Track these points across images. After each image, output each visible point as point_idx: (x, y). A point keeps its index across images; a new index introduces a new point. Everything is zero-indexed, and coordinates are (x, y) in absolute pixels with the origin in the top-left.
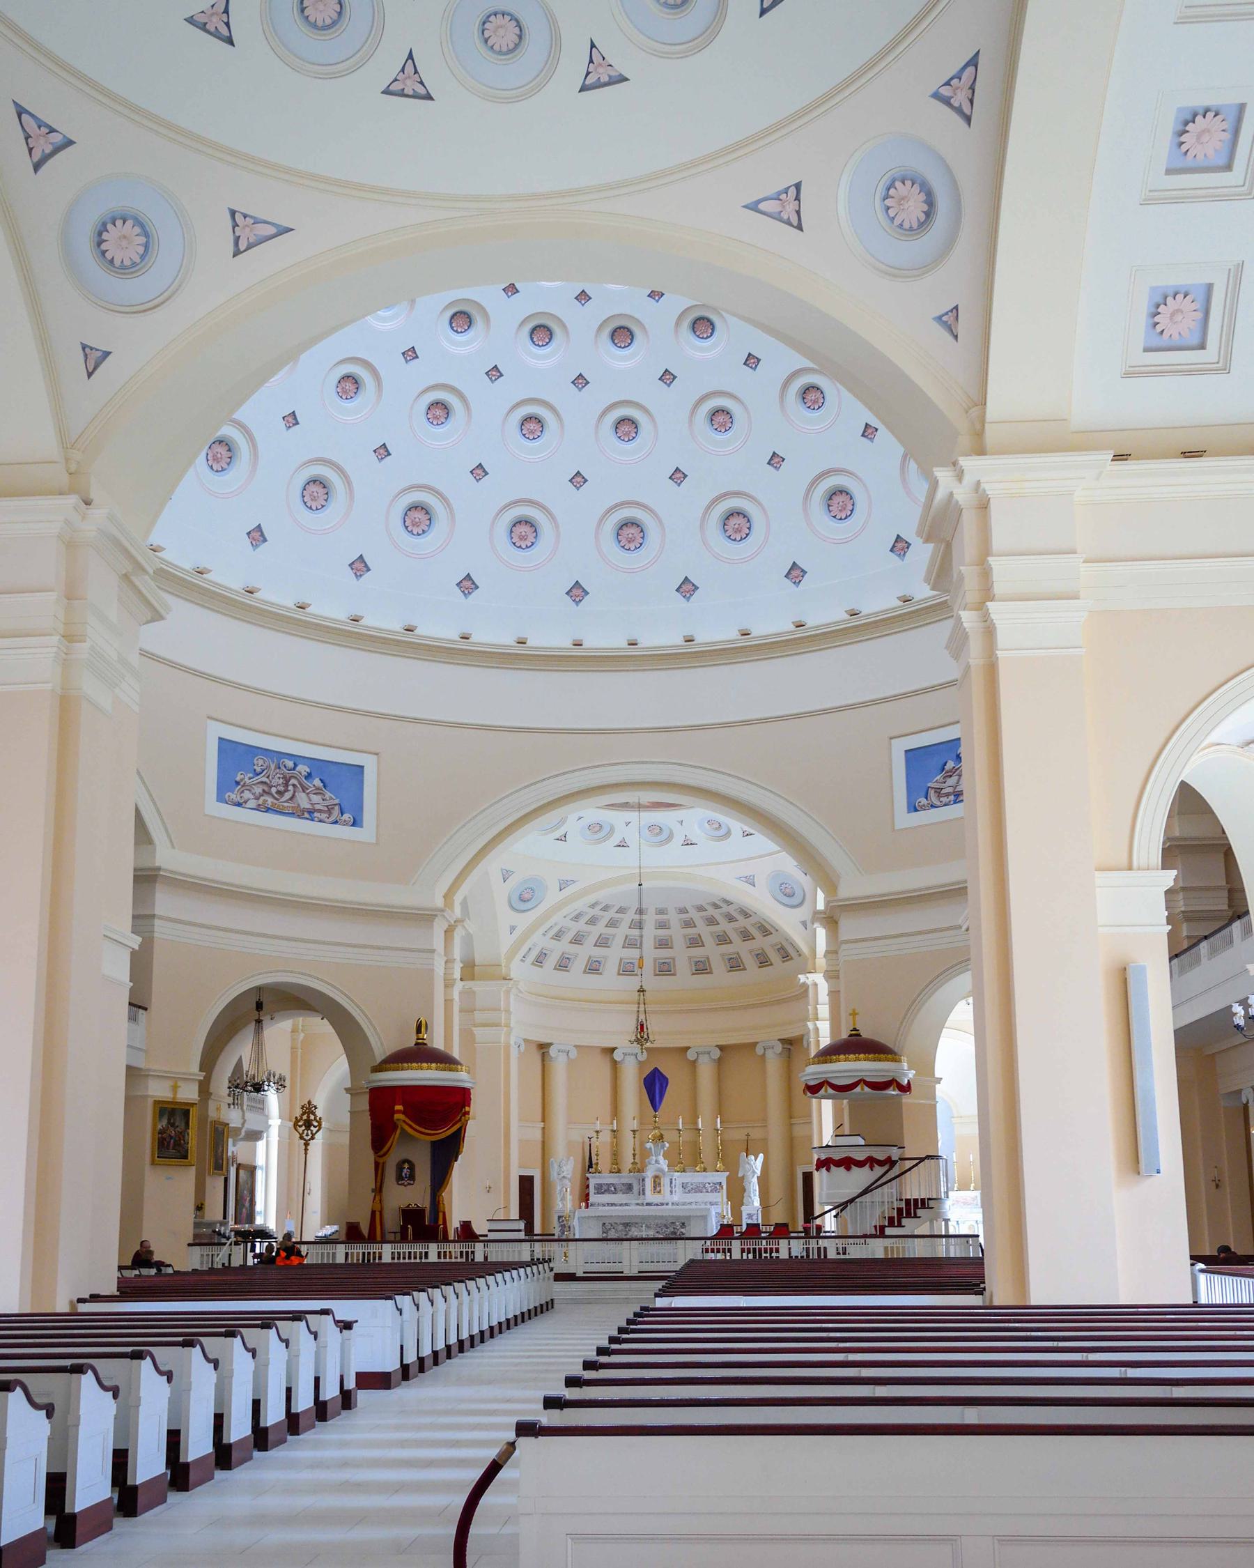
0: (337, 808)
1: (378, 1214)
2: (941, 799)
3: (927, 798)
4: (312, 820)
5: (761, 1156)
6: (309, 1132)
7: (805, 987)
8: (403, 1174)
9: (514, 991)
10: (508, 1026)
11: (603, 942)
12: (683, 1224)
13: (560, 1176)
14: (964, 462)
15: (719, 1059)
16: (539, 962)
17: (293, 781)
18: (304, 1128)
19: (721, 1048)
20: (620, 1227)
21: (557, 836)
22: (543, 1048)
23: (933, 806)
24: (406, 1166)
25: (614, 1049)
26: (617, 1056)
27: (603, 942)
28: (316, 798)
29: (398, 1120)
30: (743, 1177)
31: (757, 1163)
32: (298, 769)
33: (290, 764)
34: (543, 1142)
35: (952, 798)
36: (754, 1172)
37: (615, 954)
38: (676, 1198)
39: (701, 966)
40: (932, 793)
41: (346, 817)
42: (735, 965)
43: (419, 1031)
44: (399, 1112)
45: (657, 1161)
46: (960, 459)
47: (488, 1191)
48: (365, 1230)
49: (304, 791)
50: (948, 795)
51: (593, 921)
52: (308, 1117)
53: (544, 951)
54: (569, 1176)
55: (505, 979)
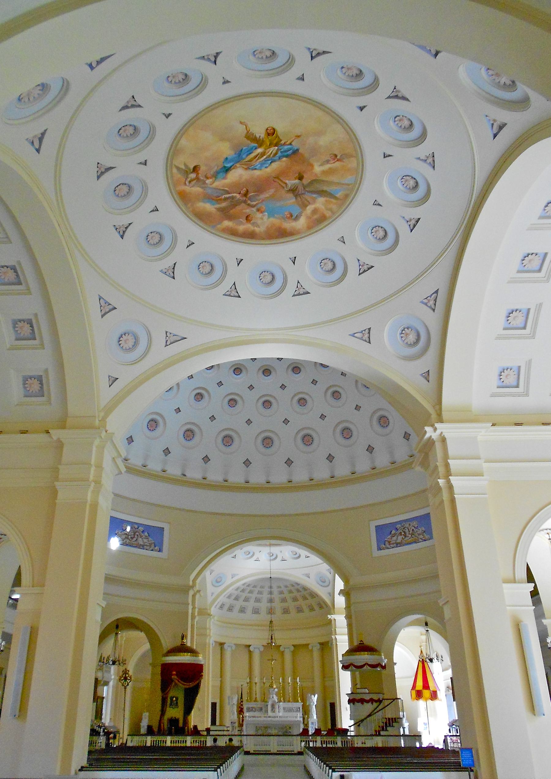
0: (153, 544)
2: (391, 545)
3: (385, 545)
4: (143, 549)
5: (316, 696)
6: (126, 682)
7: (330, 620)
9: (212, 620)
10: (210, 635)
11: (246, 600)
12: (290, 728)
14: (437, 425)
15: (294, 651)
16: (221, 607)
17: (137, 533)
18: (124, 681)
19: (294, 646)
20: (263, 729)
21: (233, 556)
23: (388, 548)
25: (250, 646)
26: (251, 649)
27: (246, 600)
28: (145, 540)
30: (309, 705)
31: (315, 698)
32: (140, 528)
33: (136, 526)
35: (395, 545)
36: (314, 703)
37: (251, 605)
38: (281, 714)
39: (285, 610)
40: (387, 543)
41: (156, 548)
42: (300, 610)
45: (273, 697)
46: (435, 424)
48: (156, 729)
49: (141, 537)
50: (393, 544)
52: (126, 675)
53: (224, 603)
55: (209, 615)
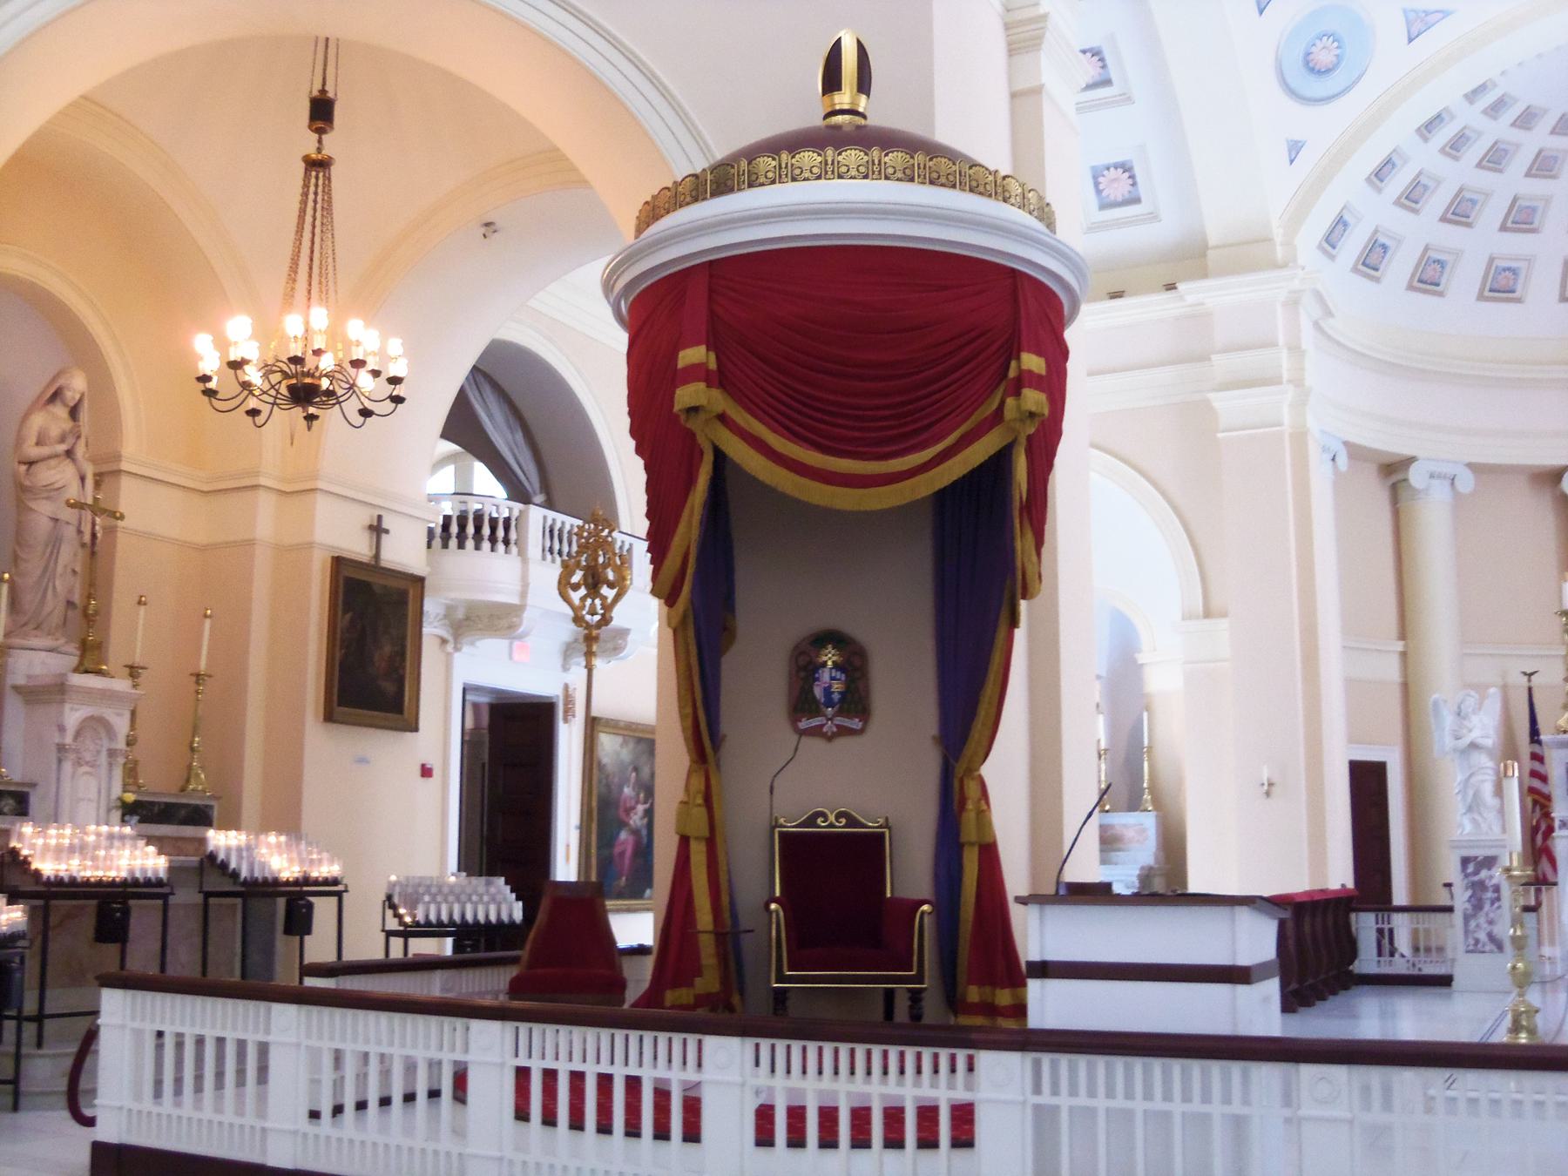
1: (698, 853)
8: (818, 692)
10: (1298, 382)
13: (1466, 741)
22: (1394, 471)
24: (830, 657)
29: (694, 410)
34: (1405, 687)
43: (832, 81)
44: (696, 373)
47: (1268, 794)
51: (1494, 159)
53: (1382, 240)
54: (1489, 742)
